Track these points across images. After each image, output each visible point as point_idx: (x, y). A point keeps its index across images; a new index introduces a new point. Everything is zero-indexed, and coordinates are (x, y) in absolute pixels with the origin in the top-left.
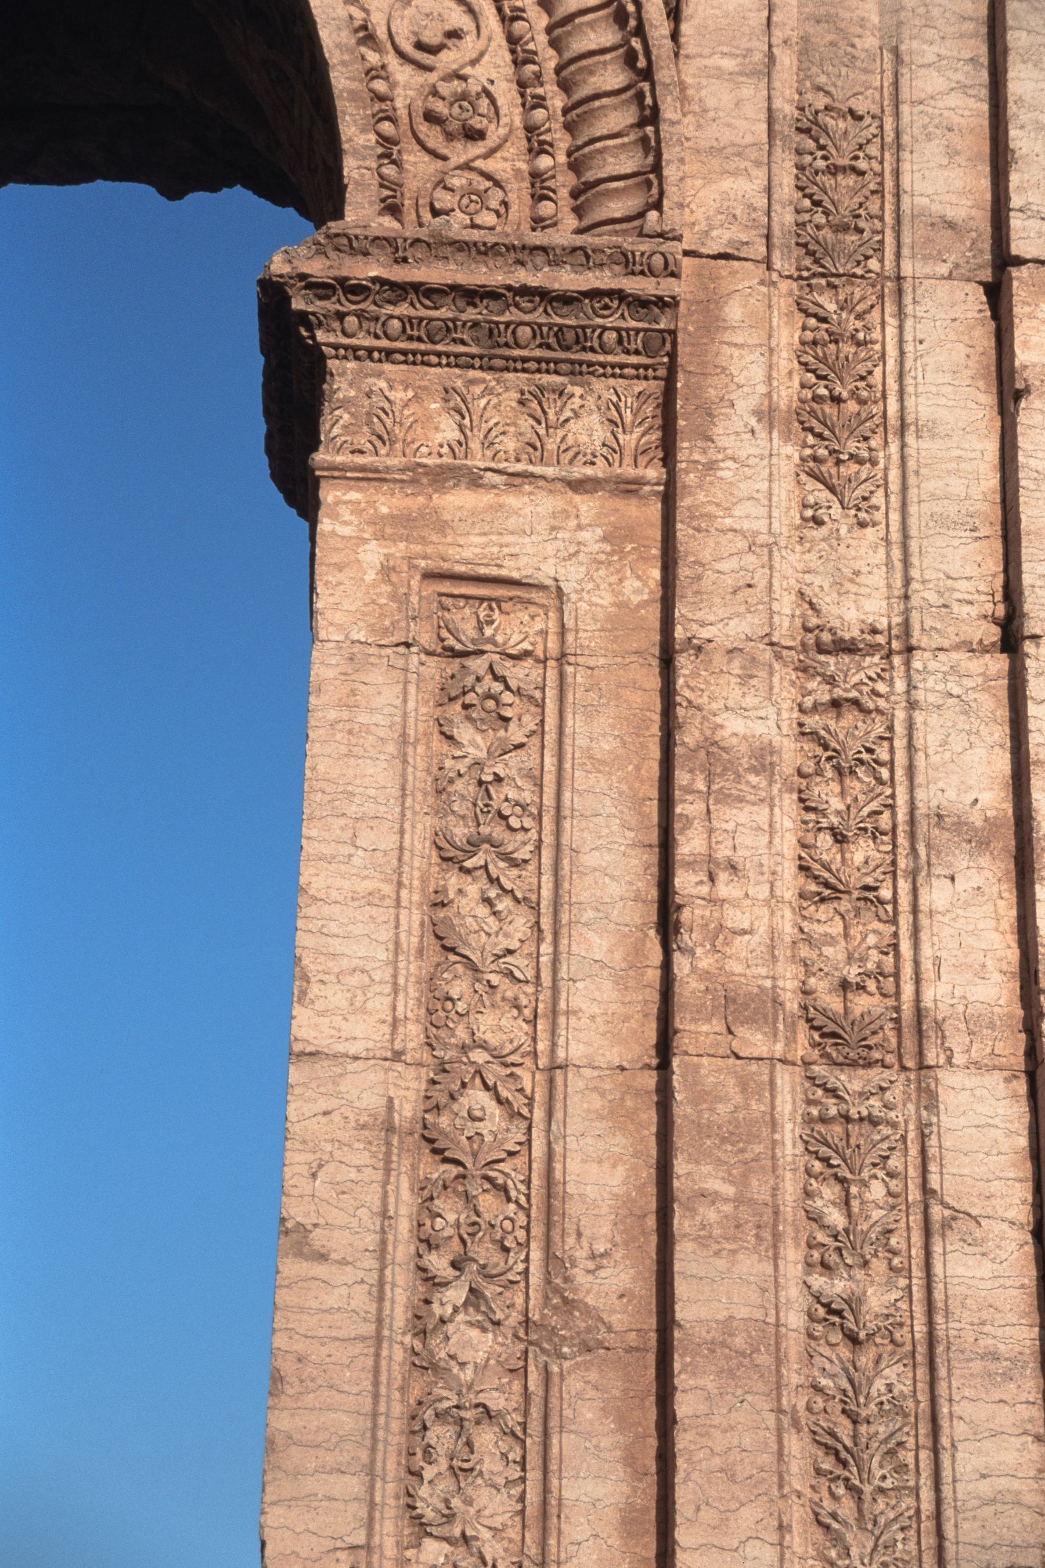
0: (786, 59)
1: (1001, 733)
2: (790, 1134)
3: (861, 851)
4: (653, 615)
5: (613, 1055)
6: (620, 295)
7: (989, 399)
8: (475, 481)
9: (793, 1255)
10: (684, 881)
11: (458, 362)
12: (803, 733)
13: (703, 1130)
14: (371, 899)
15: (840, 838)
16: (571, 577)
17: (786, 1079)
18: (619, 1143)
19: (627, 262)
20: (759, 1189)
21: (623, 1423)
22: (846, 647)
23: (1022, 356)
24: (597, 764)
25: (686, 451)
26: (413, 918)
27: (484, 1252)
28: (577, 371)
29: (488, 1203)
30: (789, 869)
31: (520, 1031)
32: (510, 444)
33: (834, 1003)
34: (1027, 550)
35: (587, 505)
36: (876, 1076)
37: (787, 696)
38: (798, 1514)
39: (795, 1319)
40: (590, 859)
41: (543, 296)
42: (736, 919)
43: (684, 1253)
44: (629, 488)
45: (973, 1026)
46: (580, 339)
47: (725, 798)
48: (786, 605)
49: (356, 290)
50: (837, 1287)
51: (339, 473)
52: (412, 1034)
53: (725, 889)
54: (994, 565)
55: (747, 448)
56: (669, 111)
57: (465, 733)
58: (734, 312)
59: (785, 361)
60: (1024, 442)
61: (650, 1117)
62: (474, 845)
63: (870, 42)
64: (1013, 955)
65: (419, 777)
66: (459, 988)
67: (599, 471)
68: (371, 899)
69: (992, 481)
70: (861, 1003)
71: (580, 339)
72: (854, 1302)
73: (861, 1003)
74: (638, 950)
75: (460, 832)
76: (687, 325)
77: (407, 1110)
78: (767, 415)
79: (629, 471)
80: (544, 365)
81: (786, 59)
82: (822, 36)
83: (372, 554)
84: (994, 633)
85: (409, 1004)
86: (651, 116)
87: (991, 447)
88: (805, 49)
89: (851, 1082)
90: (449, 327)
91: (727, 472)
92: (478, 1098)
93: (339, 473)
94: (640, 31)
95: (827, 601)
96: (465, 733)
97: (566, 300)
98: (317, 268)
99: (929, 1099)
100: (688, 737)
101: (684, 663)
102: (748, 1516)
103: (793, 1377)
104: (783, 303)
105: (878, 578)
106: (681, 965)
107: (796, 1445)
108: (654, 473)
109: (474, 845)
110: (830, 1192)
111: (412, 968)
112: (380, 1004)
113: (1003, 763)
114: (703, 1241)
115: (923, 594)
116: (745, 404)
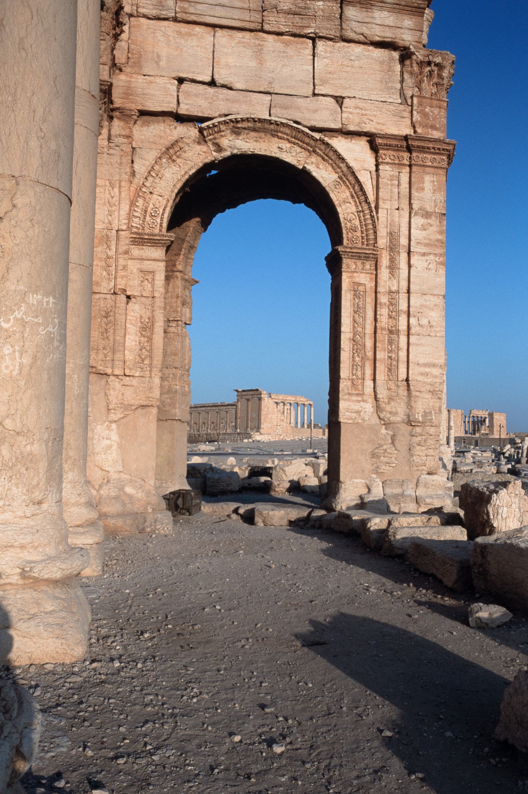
0: (389, 225)
1: (407, 302)
2: (386, 341)
3: (394, 313)
4: (374, 288)
5: (370, 333)
6: (373, 254)
7: (407, 266)
8: (357, 272)
9: (386, 352)
10: (378, 317)
11: (355, 259)
12: (389, 301)
13: (379, 341)
14: (348, 317)
15: (392, 312)
16: (366, 283)
17: (386, 336)
18: (371, 341)
19: (374, 250)
20: (384, 346)
21: (371, 366)
22: (393, 292)
23: (411, 263)
24: (369, 303)
25: (379, 271)
26: (352, 319)
27: (358, 350)
28: (367, 260)
29: (359, 346)
30: (387, 316)
31: (361, 330)
32: (360, 268)
33: (391, 328)
34: (411, 284)
35: (368, 275)
36: (394, 335)
37: (387, 297)
38: (386, 374)
39: (386, 358)
40: (368, 313)
41: (365, 253)
42: (382, 320)
43: (377, 352)
44: (372, 274)
45: (403, 331)
46: (368, 257)
47: (382, 308)
48: (387, 288)
49: (346, 252)
50: (390, 355)
51: (344, 271)
52: (352, 330)
53: (382, 317)
54: (407, 284)
55: (384, 271)
56: (378, 233)
57: (356, 299)
58: (383, 255)
59: (388, 261)
60: (411, 272)
61: (373, 339)
62: (357, 311)
63: (397, 224)
64: (407, 324)
65: (352, 304)
66: (356, 326)
67: (369, 272)
68: (348, 317)
69: (407, 275)
70: (393, 328)
71: (368, 257)
72: (391, 356)
73: (393, 328)
74: (372, 323)
75: (356, 310)
76: (379, 257)
77: (352, 337)
78: (386, 267)
79: (372, 272)
80: (364, 260)
81: (389, 225)
82: (392, 223)
83: (347, 280)
84: (406, 291)
85: (352, 327)
86: (375, 232)
87: (407, 271)
88: (391, 224)
89: (392, 336)
90: (355, 256)
91: (382, 273)
92: (358, 336)
93: (344, 271)
94: (375, 222)
95: (391, 287)
96: (356, 299)
97: (367, 254)
98: (343, 250)
99: (399, 338)
100: (378, 302)
101: (378, 294)
102: (382, 375)
103: (386, 363)
104: (388, 254)
105: (396, 285)
106: (377, 325)
107: (386, 369)
108: (375, 272)
109: (357, 311)
110: (390, 346)
111: (352, 323)
112: (349, 327)
113: (407, 305)
114: (379, 351)
115: (400, 287)
116: (384, 266)
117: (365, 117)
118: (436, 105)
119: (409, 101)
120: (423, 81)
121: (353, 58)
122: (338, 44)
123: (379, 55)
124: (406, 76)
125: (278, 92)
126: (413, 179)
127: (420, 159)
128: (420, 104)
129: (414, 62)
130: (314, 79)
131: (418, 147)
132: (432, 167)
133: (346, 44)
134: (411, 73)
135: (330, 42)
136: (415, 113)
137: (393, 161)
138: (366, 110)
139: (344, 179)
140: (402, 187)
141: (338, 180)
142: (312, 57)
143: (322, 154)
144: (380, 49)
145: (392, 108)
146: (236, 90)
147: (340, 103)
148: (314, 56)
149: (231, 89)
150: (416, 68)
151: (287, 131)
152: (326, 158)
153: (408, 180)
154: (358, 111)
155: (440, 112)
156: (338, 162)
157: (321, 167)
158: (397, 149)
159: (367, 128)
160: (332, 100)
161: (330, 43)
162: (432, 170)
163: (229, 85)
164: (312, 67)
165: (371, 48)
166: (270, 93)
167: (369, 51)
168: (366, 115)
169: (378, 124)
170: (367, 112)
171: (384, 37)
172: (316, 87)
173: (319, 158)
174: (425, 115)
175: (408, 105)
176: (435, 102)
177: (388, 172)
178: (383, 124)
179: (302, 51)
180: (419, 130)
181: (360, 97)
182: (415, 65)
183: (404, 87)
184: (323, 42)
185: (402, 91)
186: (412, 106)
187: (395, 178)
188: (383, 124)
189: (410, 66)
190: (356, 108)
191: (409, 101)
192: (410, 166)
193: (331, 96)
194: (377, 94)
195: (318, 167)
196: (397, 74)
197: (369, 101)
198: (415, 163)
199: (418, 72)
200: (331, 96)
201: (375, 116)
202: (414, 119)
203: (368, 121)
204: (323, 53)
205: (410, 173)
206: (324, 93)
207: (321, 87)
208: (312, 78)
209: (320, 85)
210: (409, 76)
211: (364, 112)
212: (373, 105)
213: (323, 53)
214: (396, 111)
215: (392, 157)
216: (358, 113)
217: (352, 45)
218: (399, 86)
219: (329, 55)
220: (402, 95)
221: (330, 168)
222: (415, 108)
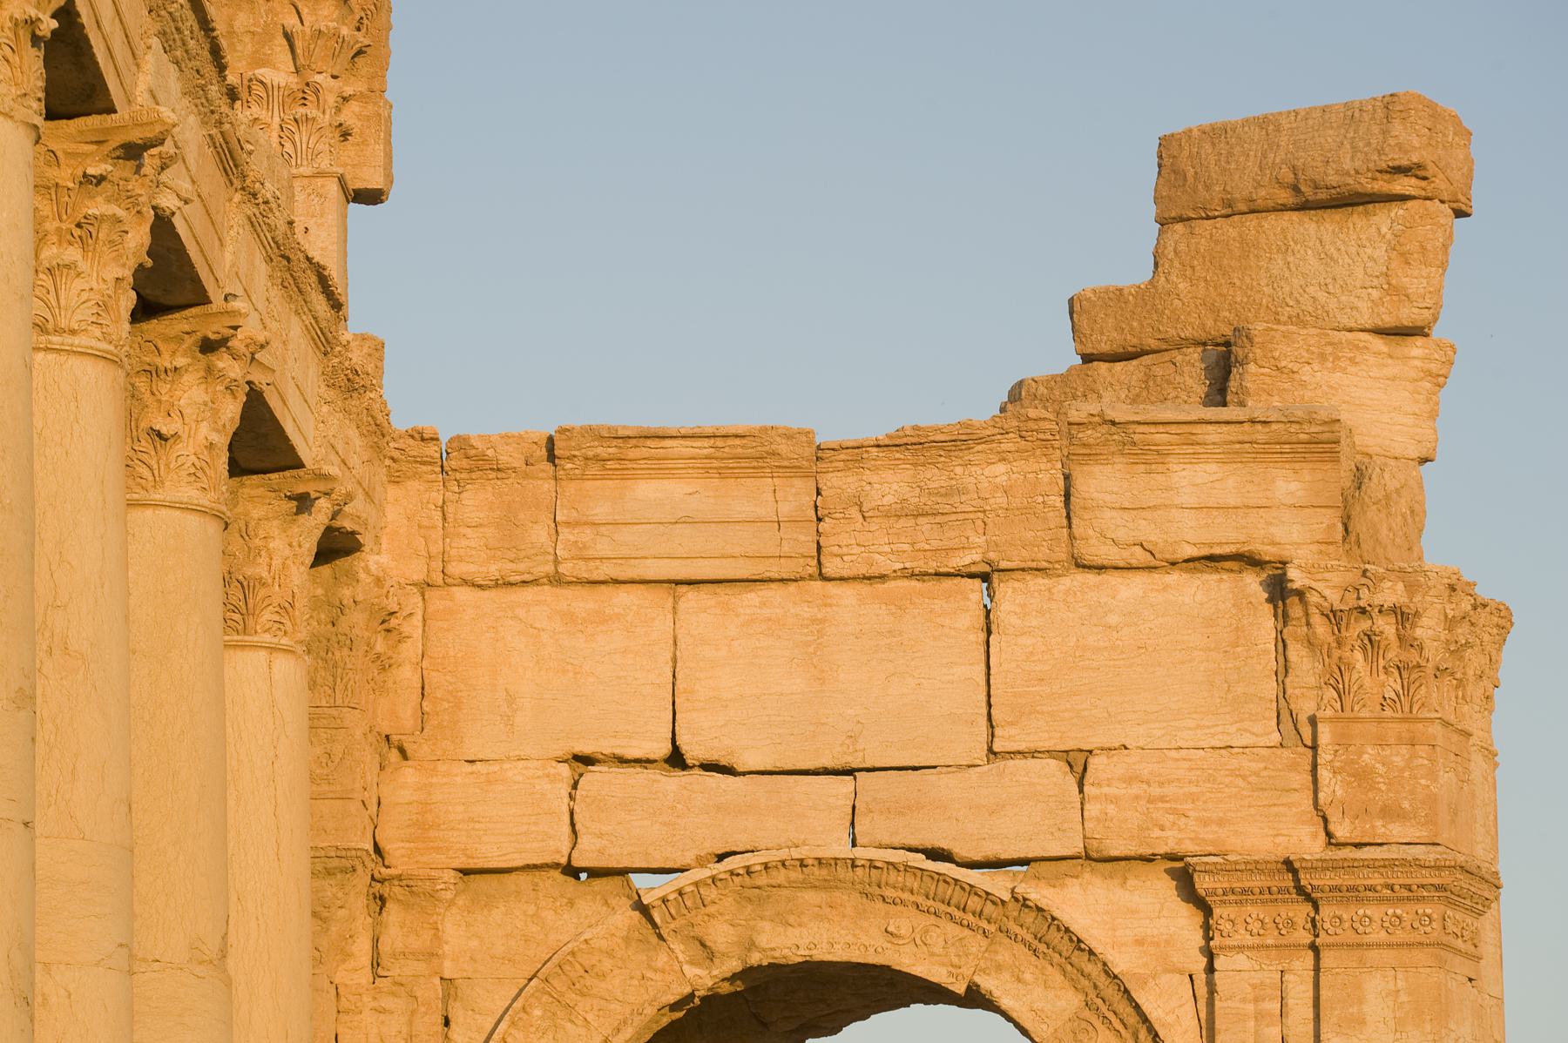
117: (1160, 805)
118: (1399, 738)
119: (1307, 732)
120: (1351, 667)
121: (1113, 619)
122: (1062, 580)
123: (1199, 597)
124: (1296, 652)
125: (878, 765)
126: (1325, 994)
127: (1347, 925)
128: (1342, 742)
129: (1312, 610)
130: (990, 705)
131: (1333, 889)
132: (1390, 946)
133: (1091, 578)
134: (1310, 643)
135: (1041, 581)
136: (1324, 774)
137: (1257, 940)
138: (1161, 784)
139: (1104, 1009)
140: (1289, 1021)
141: (1087, 1014)
142: (983, 636)
143: (1029, 937)
144: (1206, 577)
145: (1248, 764)
146: (744, 774)
147: (1079, 769)
148: (989, 632)
149: (728, 770)
150: (1321, 628)
151: (911, 881)
152: (1042, 947)
153: (1310, 994)
154: (1136, 789)
155: (1414, 756)
156: (1081, 959)
157: (1028, 976)
158: (1268, 895)
159: (1169, 842)
160: (1054, 766)
161: (1041, 582)
162: (1389, 956)
163: (724, 762)
164: (983, 666)
165: (1175, 577)
166: (850, 772)
167: (1166, 588)
168: (1162, 799)
169: (1205, 823)
170: (1169, 790)
171: (1211, 545)
172: (998, 731)
173: (1021, 950)
174: (1362, 777)
175: (1305, 746)
176: (1393, 729)
177: (1245, 975)
178: (1221, 823)
179: (947, 622)
180: (1341, 831)
181: (1141, 744)
182: (1316, 619)
183: (1289, 691)
184: (1016, 585)
185: (1282, 701)
186: (1314, 748)
187: (1269, 991)
188: (1221, 823)
189: (1304, 620)
190: (1130, 780)
191: (1307, 732)
192: (1314, 948)
193: (1050, 753)
194: (1198, 727)
195: (1019, 980)
196: (1266, 652)
197: (1173, 754)
198: (1330, 940)
199: (1331, 639)
200: (1050, 753)
201: (1194, 798)
202: (1321, 795)
203: (1171, 817)
204: (1014, 620)
205: (1317, 969)
206: (1023, 747)
207: (1013, 731)
208: (984, 704)
209: (1011, 724)
210: (1304, 652)
211: (1156, 791)
212: (1186, 765)
213: (1014, 620)
214: (1264, 773)
215: (1255, 927)
216: (1137, 797)
217: (1112, 578)
218: (1270, 688)
219: (1034, 623)
220: (1285, 715)
221: (1058, 977)
222: (1324, 757)
